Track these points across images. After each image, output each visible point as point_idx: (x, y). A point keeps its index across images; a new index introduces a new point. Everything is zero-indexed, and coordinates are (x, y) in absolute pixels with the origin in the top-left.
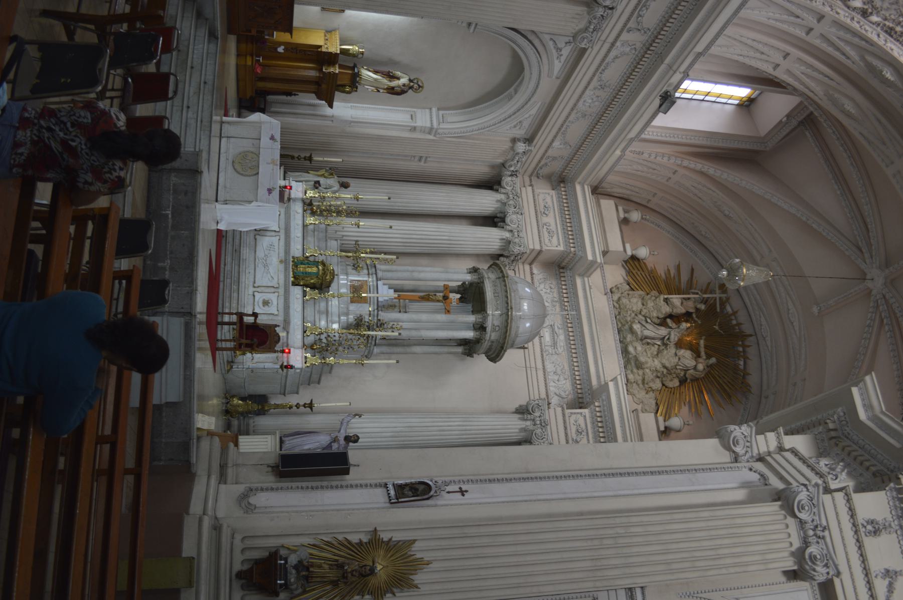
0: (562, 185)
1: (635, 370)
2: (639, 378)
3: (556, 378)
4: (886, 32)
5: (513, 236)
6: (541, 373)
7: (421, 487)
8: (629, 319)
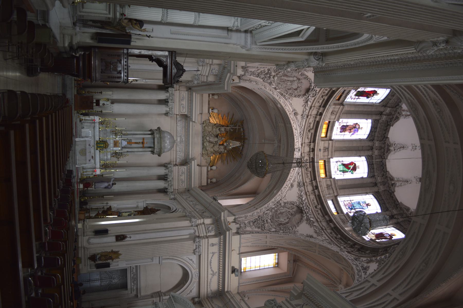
0: (190, 91)
1: (205, 151)
2: (206, 153)
3: (180, 153)
4: (281, 94)
5: (170, 111)
6: (175, 152)
7: (122, 237)
8: (206, 134)
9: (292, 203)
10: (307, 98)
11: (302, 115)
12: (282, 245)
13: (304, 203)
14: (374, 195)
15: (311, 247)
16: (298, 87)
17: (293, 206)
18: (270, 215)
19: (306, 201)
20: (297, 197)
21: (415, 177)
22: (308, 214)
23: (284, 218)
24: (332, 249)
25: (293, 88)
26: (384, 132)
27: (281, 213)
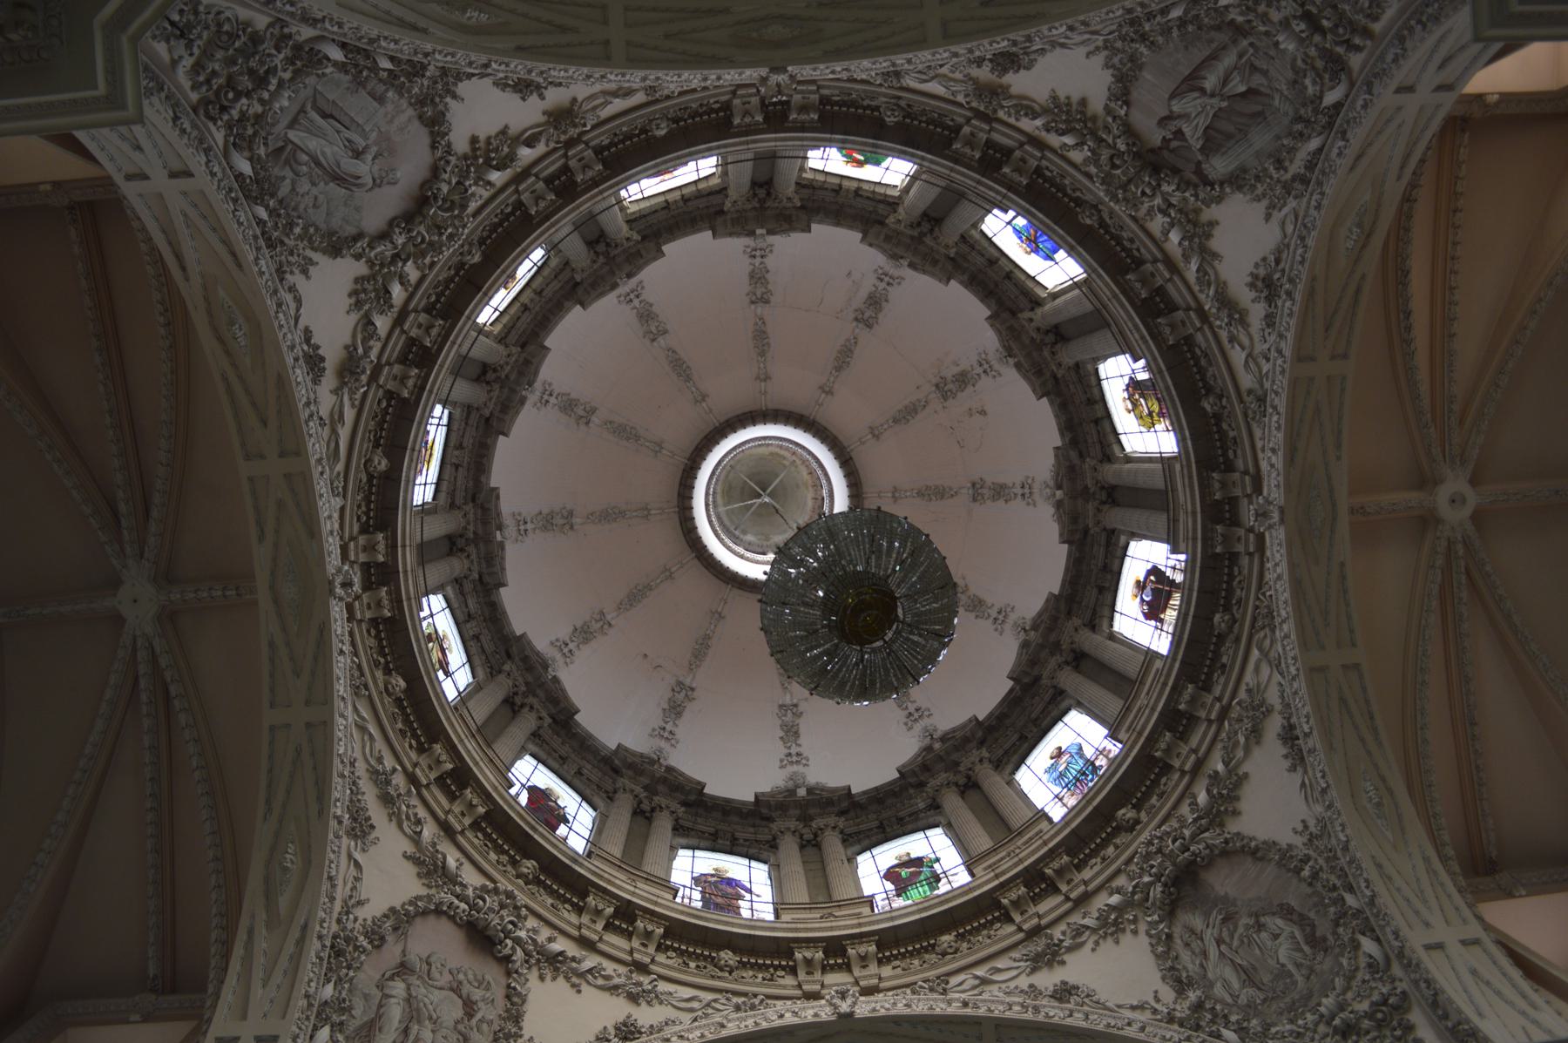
9: (1164, 949)
10: (527, 953)
11: (634, 998)
12: (1426, 860)
13: (1135, 887)
14: (1009, 768)
15: (1343, 700)
16: (456, 989)
17: (1178, 941)
18: (1288, 1027)
19: (1121, 881)
20: (1117, 942)
21: (910, 729)
22: (1187, 833)
23: (1269, 943)
24: (1283, 569)
25: (457, 1022)
26: (735, 819)
27: (1249, 976)
